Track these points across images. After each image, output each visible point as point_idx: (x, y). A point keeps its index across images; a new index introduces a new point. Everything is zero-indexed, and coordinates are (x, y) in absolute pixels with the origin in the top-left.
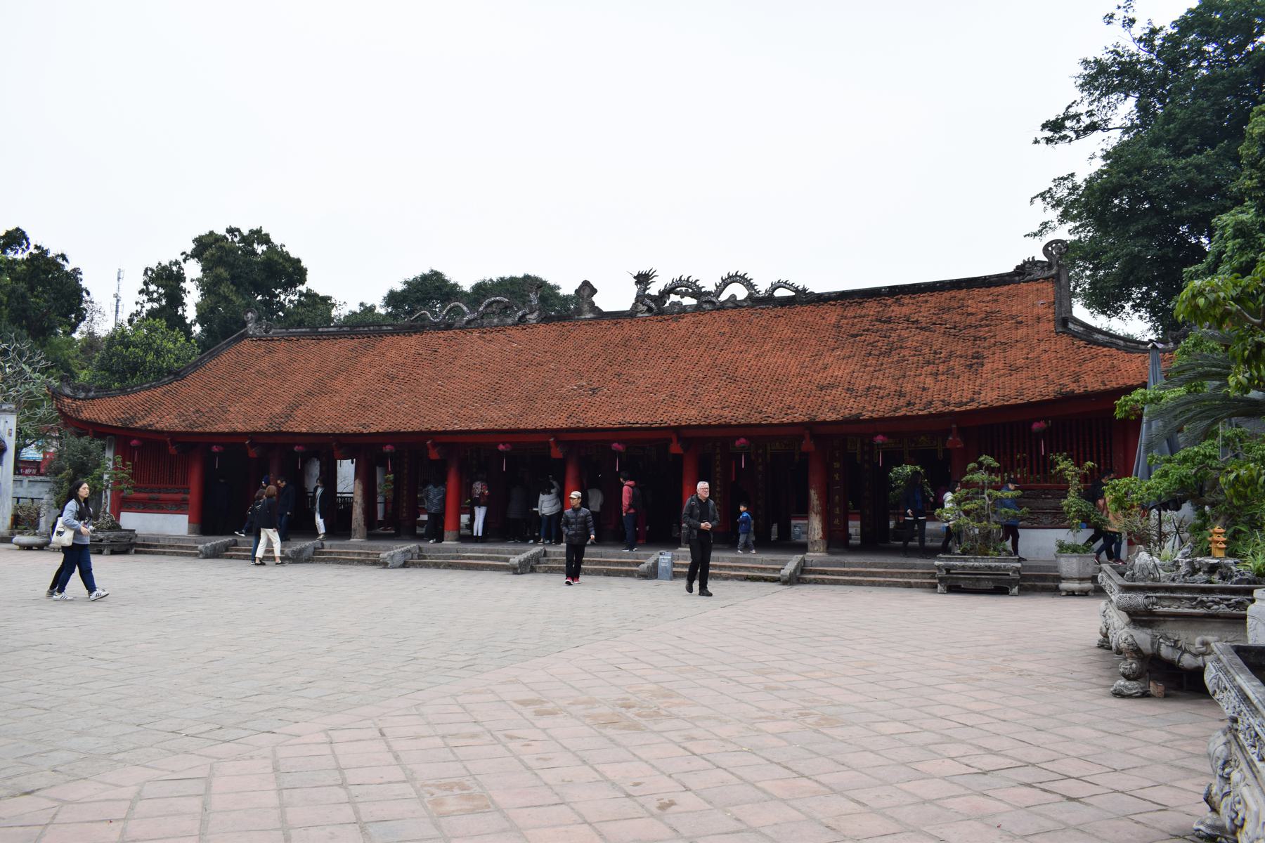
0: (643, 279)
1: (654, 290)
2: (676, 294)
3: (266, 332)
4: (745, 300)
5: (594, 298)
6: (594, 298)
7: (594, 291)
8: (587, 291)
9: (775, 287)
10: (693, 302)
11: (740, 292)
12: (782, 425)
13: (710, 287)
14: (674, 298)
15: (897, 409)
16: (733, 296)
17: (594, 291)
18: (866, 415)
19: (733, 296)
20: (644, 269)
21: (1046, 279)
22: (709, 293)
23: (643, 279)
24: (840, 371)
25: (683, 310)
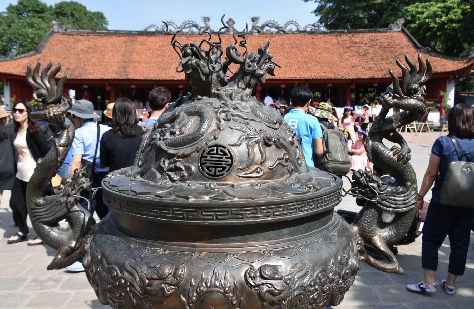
0: (254, 20)
1: (260, 24)
2: (268, 26)
3: (66, 30)
4: (296, 31)
5: (234, 26)
6: (235, 26)
7: (234, 23)
8: (231, 23)
9: (307, 27)
10: (276, 30)
11: (294, 29)
12: (349, 79)
13: (282, 24)
14: (267, 28)
15: (385, 75)
16: (291, 29)
17: (234, 23)
18: (376, 77)
19: (291, 29)
20: (255, 15)
21: (399, 31)
22: (281, 27)
23: (254, 20)
24: (355, 61)
25: (272, 33)
